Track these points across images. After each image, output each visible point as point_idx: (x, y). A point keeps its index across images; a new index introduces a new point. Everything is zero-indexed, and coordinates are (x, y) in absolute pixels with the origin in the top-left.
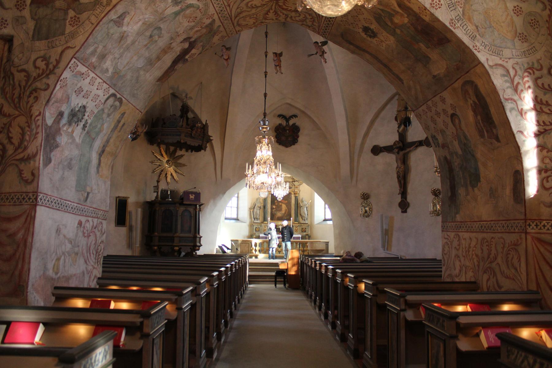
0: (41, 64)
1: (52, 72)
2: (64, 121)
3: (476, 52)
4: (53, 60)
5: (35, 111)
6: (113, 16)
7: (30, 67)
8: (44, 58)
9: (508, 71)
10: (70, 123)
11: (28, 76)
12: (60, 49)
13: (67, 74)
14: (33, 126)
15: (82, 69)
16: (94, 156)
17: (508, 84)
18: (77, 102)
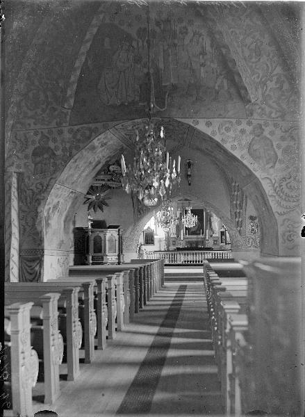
0: (41, 187)
1: (45, 190)
2: (51, 210)
3: (254, 172)
4: (45, 185)
5: (39, 211)
6: (72, 160)
7: (33, 187)
8: (41, 184)
9: (271, 180)
10: (53, 212)
11: (33, 193)
12: (48, 179)
13: (52, 191)
14: (39, 217)
15: (58, 186)
16: (62, 222)
17: (271, 188)
18: (56, 201)
